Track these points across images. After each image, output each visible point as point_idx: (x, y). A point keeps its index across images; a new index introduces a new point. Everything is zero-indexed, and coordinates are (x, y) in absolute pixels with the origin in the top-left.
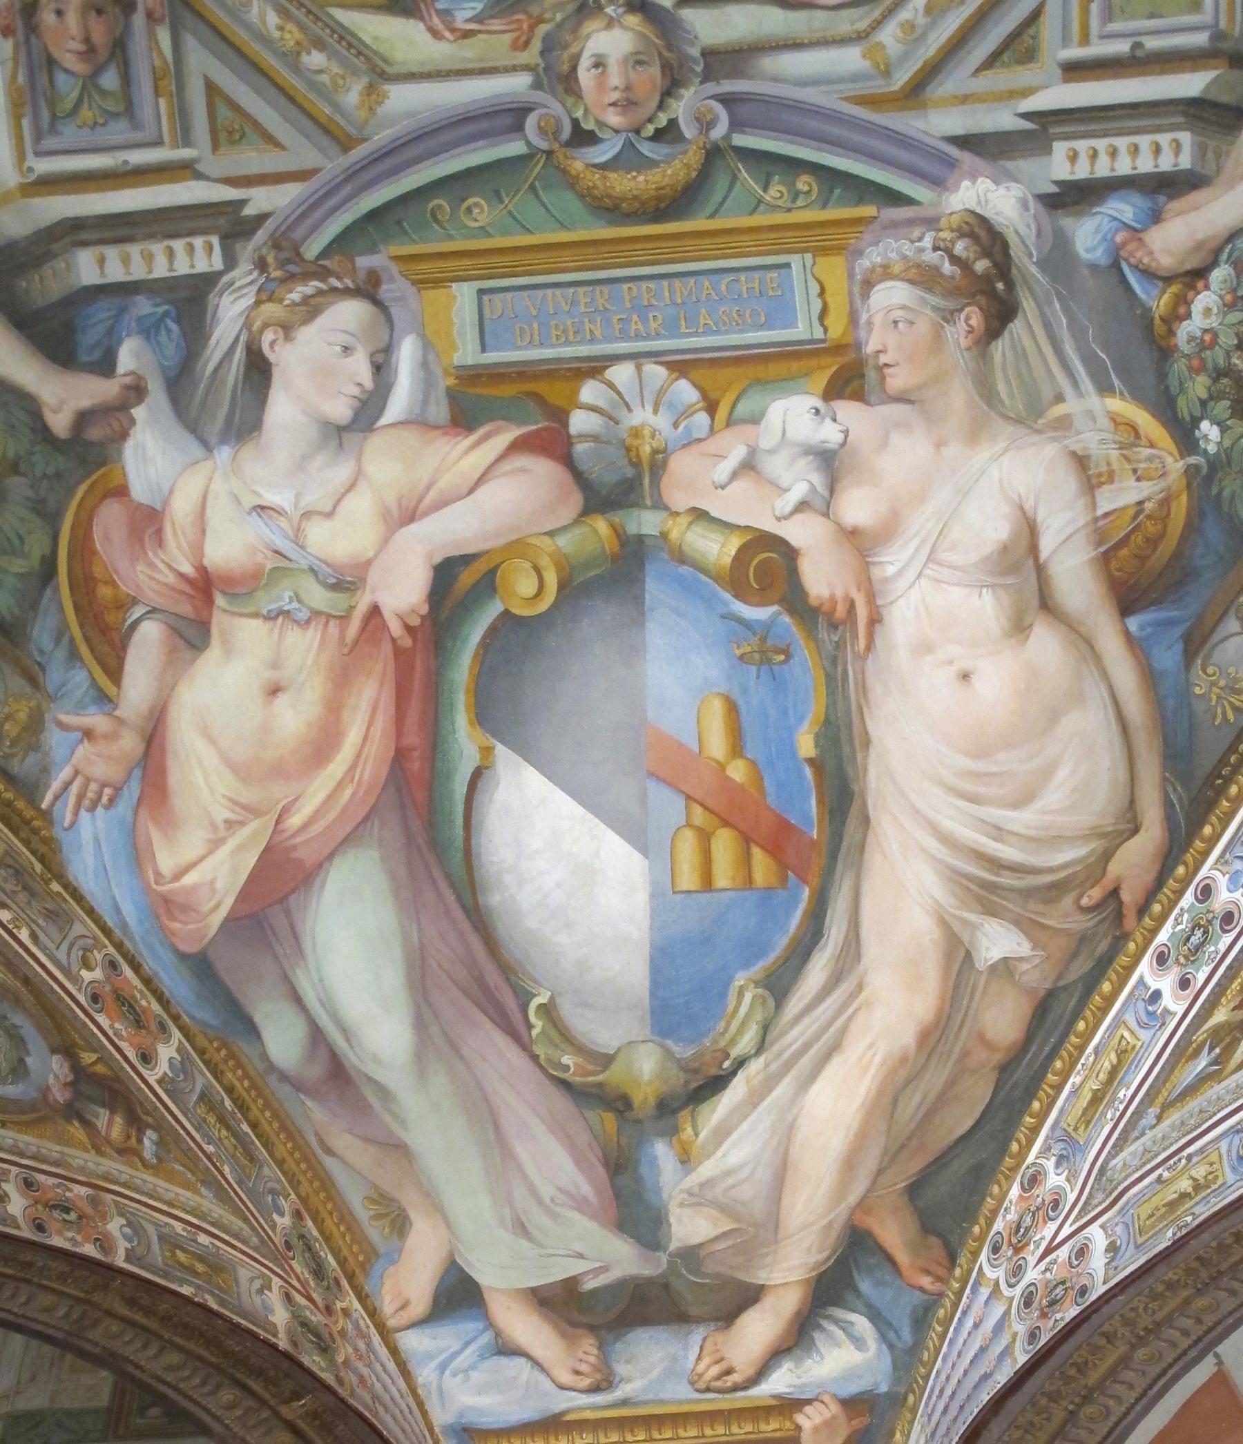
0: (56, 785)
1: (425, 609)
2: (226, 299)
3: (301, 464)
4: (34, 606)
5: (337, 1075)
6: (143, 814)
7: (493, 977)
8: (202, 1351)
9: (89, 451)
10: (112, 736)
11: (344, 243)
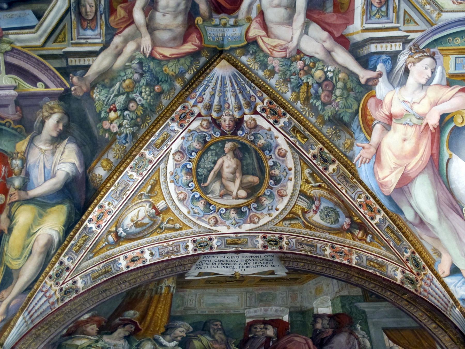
0: (356, 158)
1: (438, 124)
2: (402, 56)
3: (414, 92)
4: (353, 119)
5: (422, 223)
6: (376, 165)
7: (454, 203)
8: (378, 284)
9: (368, 87)
10: (369, 148)
11: (428, 46)
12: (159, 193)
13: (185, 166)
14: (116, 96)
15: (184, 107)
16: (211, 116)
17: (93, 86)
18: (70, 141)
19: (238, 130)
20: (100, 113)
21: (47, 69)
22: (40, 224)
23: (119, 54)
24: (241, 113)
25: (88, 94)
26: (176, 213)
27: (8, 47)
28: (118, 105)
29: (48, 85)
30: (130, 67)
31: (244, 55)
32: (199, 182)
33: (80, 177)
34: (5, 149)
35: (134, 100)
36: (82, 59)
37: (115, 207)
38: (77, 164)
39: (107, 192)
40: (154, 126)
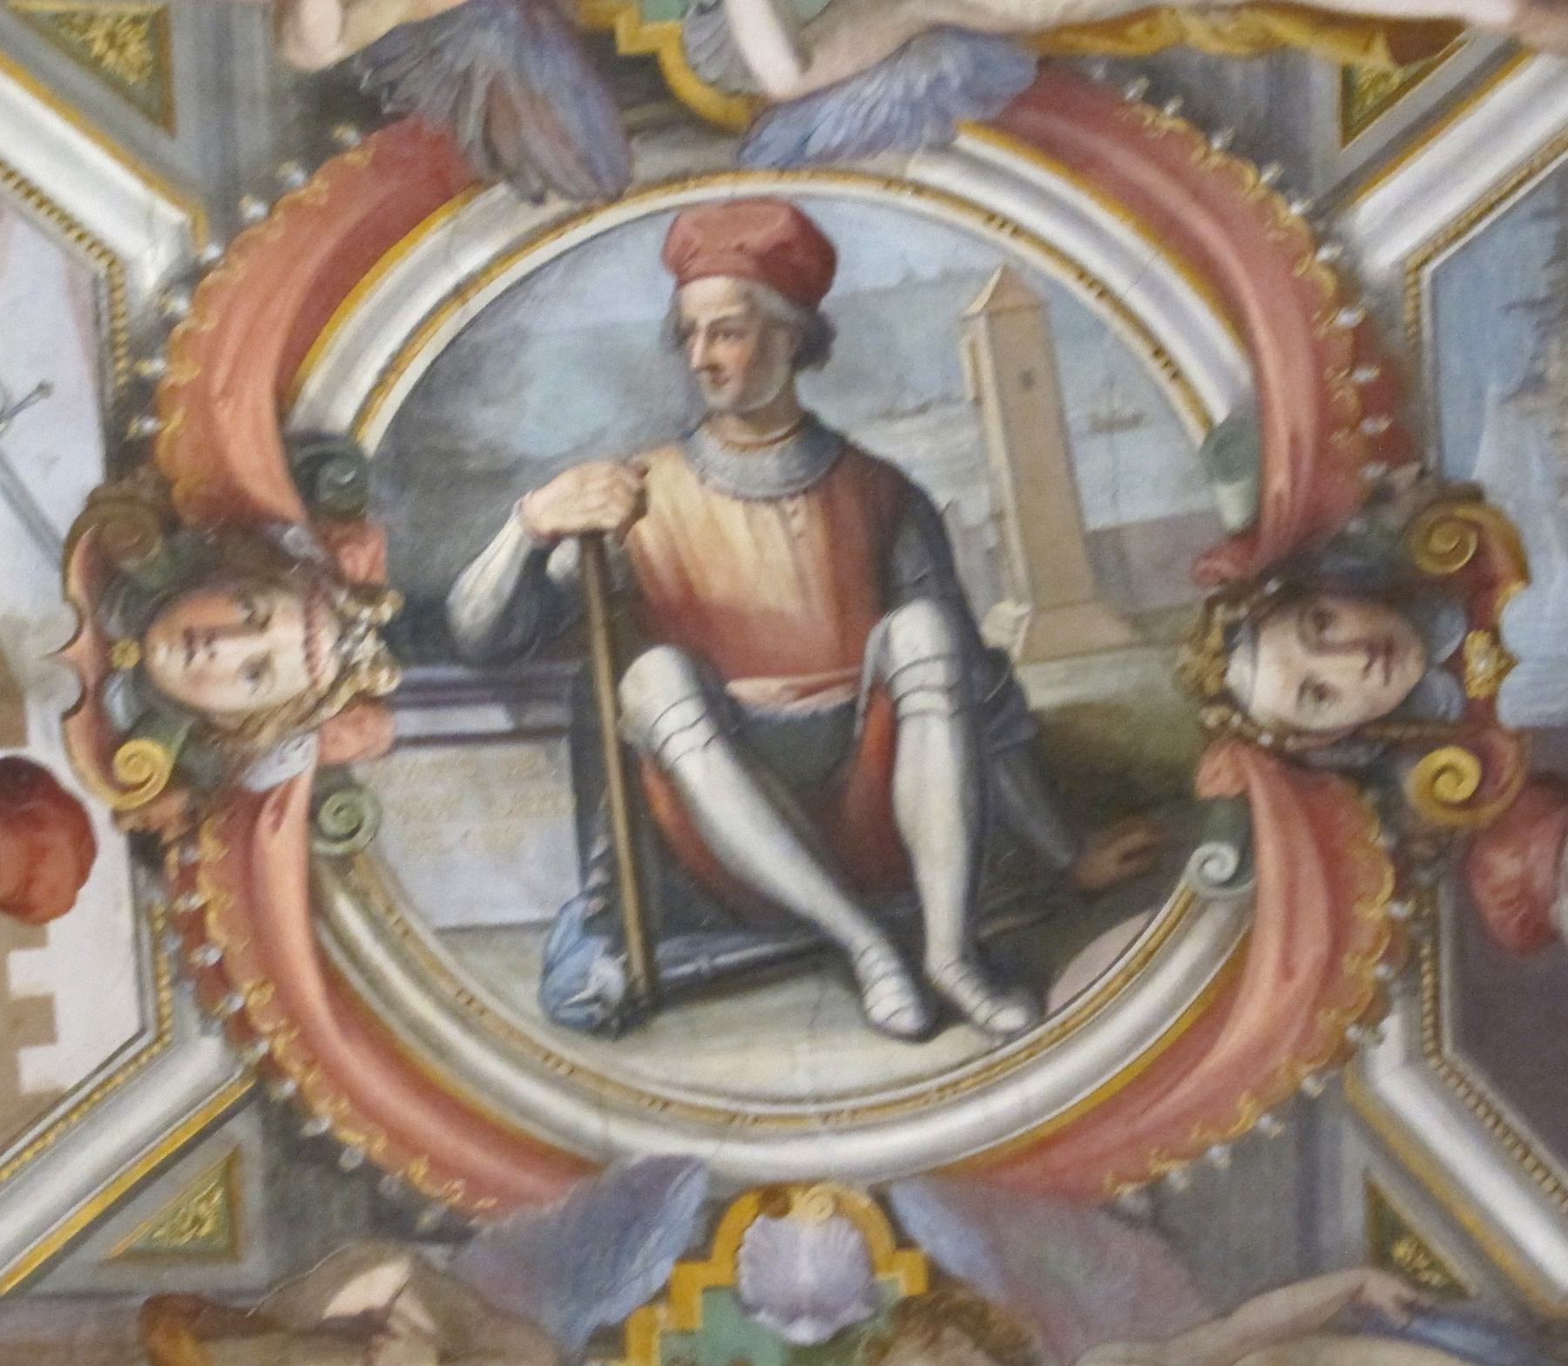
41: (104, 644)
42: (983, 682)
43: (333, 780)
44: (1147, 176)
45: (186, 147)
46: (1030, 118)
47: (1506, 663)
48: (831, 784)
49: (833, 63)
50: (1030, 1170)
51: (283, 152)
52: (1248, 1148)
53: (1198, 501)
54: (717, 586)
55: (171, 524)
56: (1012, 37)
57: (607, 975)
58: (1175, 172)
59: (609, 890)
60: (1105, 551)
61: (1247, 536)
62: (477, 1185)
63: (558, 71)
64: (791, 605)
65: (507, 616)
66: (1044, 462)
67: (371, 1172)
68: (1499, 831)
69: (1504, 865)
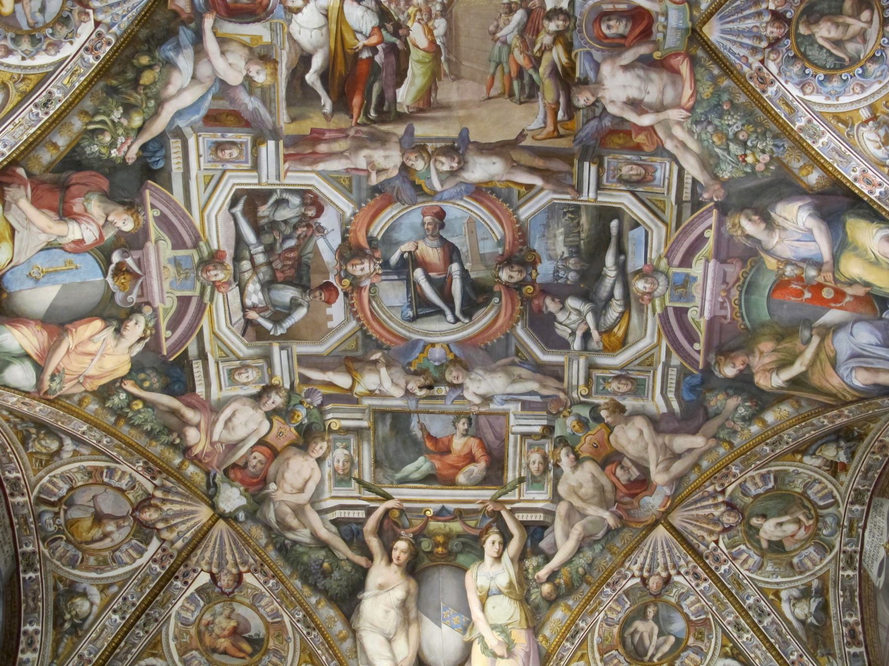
12: (850, 114)
13: (820, 82)
14: (729, 153)
15: (751, 78)
16: (764, 49)
17: (715, 177)
18: (773, 209)
19: (785, 17)
20: (746, 173)
21: (691, 224)
22: (866, 250)
23: (684, 145)
24: (765, 13)
25: (724, 183)
26: (877, 98)
27: (664, 262)
28: (740, 152)
29: (708, 225)
30: (699, 135)
31: (699, 6)
32: (843, 67)
33: (816, 202)
34: (772, 281)
35: (736, 134)
36: (685, 185)
37: (859, 165)
38: (800, 203)
39: (838, 171)
40: (769, 112)
41: (341, 266)
42: (464, 274)
43: (373, 285)
44: (490, 204)
45: (354, 196)
46: (474, 195)
47: (538, 274)
48: (443, 288)
49: (445, 187)
50: (469, 342)
51: (368, 197)
52: (499, 340)
53: (496, 250)
54: (427, 259)
55: (350, 249)
56: (472, 184)
57: (410, 313)
58: (494, 204)
59: (411, 302)
60: (482, 257)
61: (502, 255)
62: (391, 342)
63: (407, 186)
64: (438, 262)
65: (398, 263)
66: (474, 245)
67: (377, 340)
68: (536, 297)
69: (536, 302)
